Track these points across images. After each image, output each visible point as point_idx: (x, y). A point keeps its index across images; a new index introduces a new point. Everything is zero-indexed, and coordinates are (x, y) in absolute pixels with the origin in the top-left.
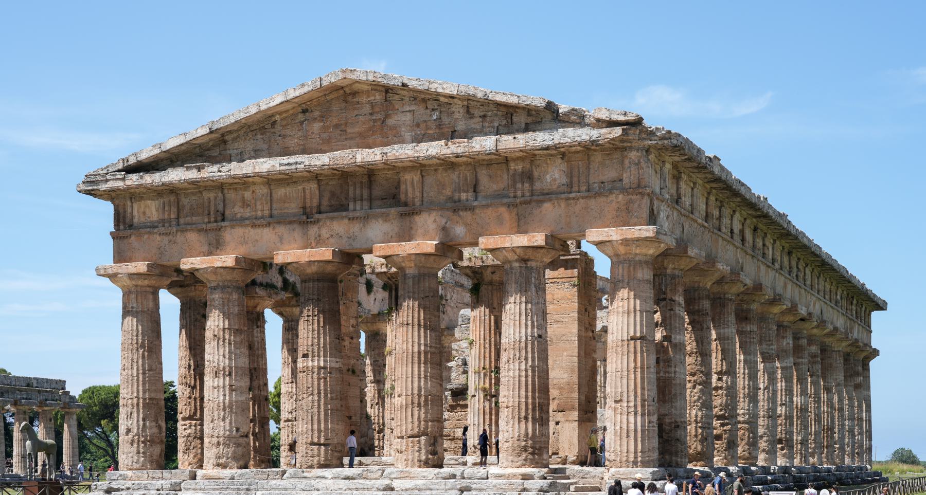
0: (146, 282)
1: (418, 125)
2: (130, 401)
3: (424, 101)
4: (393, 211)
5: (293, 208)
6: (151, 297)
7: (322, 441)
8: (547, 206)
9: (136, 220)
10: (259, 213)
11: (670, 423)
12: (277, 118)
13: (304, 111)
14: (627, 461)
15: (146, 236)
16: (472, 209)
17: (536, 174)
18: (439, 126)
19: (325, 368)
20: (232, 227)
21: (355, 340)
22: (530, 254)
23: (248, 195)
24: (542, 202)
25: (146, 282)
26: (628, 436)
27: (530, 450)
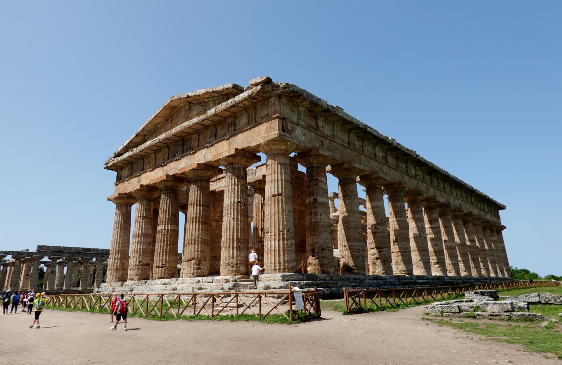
0: (121, 201)
3: (201, 103)
6: (125, 207)
7: (160, 266)
11: (319, 248)
12: (159, 126)
14: (271, 269)
17: (237, 122)
19: (165, 230)
21: (220, 223)
22: (231, 160)
25: (121, 201)
26: (271, 254)
27: (231, 265)
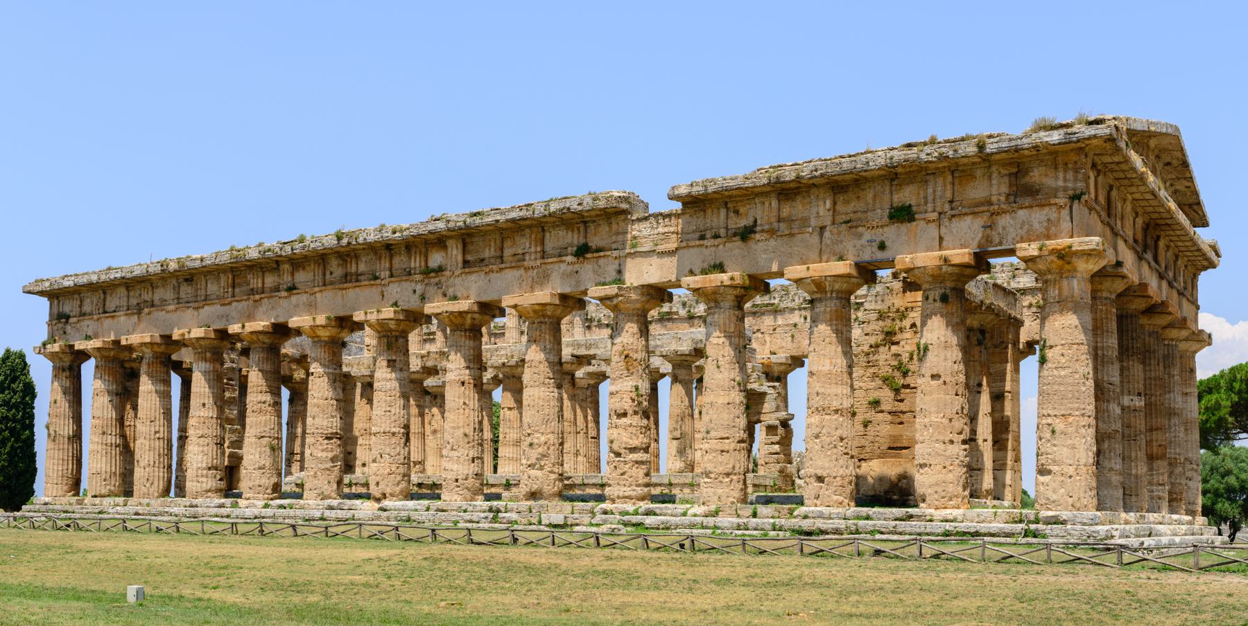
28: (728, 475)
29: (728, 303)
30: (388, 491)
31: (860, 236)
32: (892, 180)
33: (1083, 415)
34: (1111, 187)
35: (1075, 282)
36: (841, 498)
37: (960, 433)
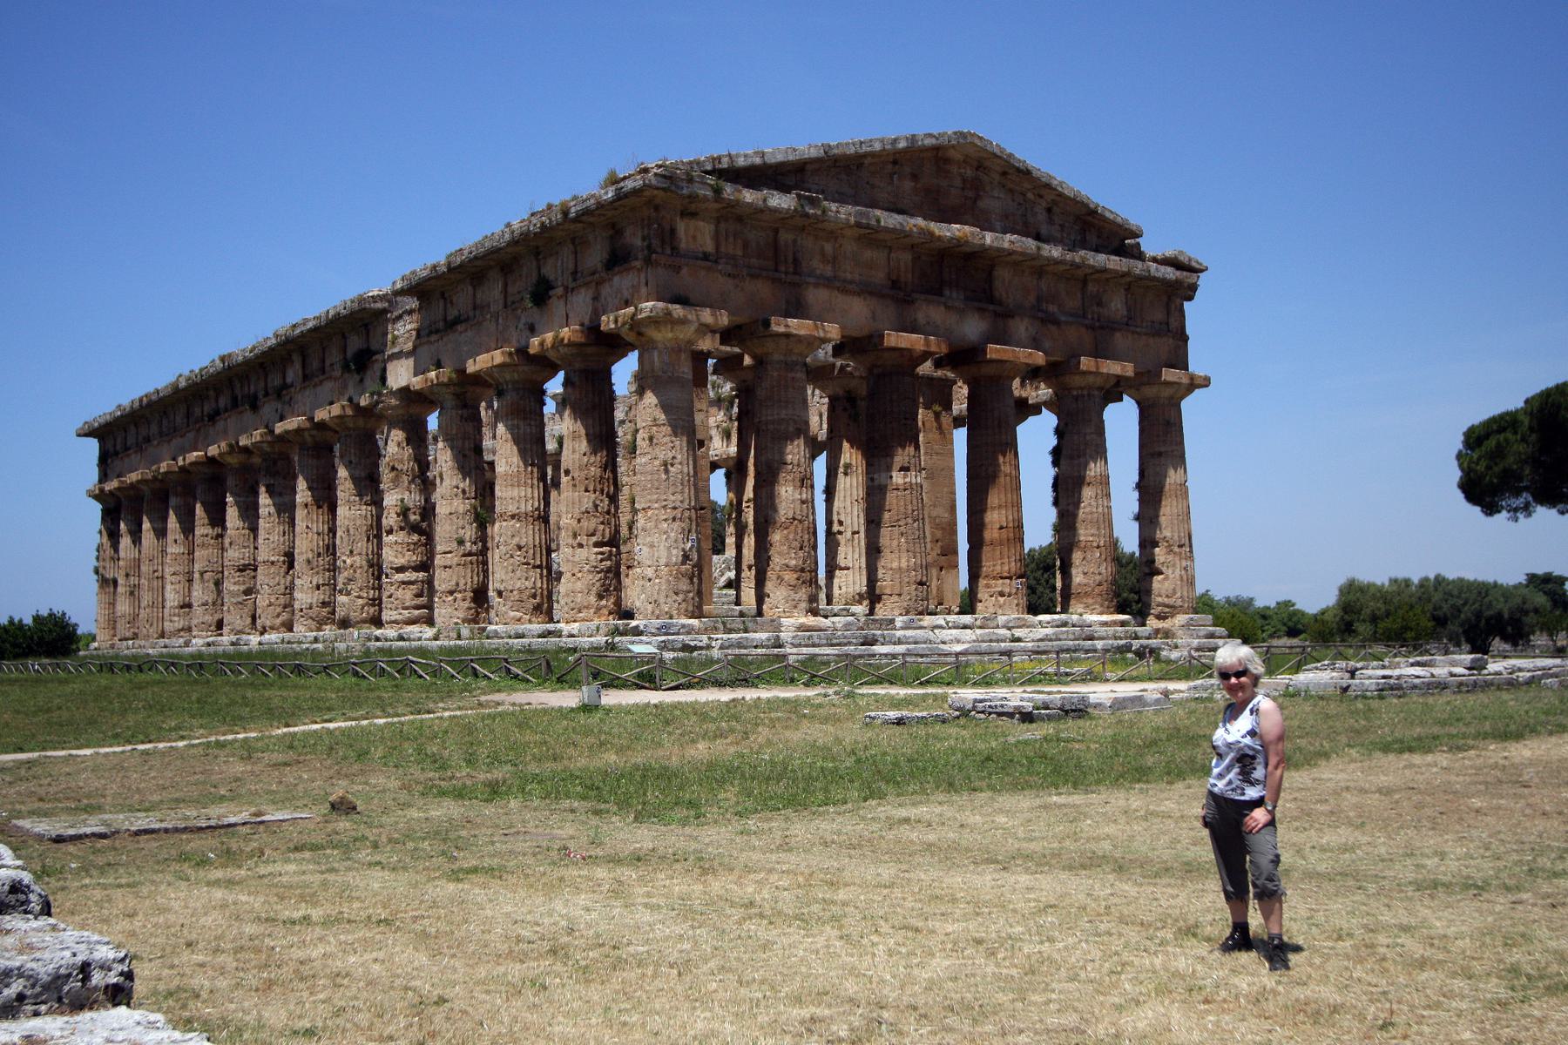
1: (1007, 217)
2: (687, 514)
3: (1011, 191)
4: (991, 307)
5: (879, 277)
8: (1118, 335)
9: (683, 245)
10: (849, 276)
13: (895, 162)
15: (703, 273)
16: (1057, 323)
18: (1026, 224)
20: (816, 285)
23: (828, 247)
24: (1114, 330)
28: (451, 593)
29: (450, 402)
30: (268, 623)
31: (519, 318)
32: (538, 254)
33: (664, 507)
34: (776, 231)
35: (656, 353)
36: (519, 614)
37: (593, 535)
